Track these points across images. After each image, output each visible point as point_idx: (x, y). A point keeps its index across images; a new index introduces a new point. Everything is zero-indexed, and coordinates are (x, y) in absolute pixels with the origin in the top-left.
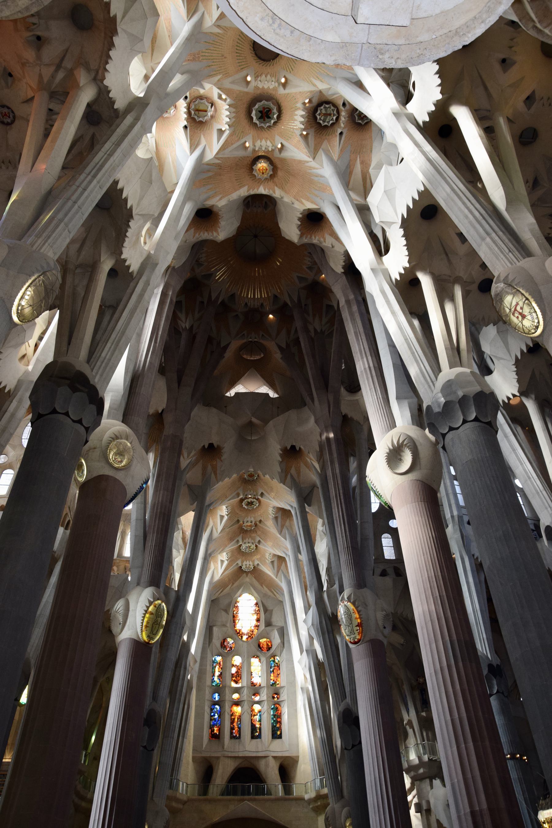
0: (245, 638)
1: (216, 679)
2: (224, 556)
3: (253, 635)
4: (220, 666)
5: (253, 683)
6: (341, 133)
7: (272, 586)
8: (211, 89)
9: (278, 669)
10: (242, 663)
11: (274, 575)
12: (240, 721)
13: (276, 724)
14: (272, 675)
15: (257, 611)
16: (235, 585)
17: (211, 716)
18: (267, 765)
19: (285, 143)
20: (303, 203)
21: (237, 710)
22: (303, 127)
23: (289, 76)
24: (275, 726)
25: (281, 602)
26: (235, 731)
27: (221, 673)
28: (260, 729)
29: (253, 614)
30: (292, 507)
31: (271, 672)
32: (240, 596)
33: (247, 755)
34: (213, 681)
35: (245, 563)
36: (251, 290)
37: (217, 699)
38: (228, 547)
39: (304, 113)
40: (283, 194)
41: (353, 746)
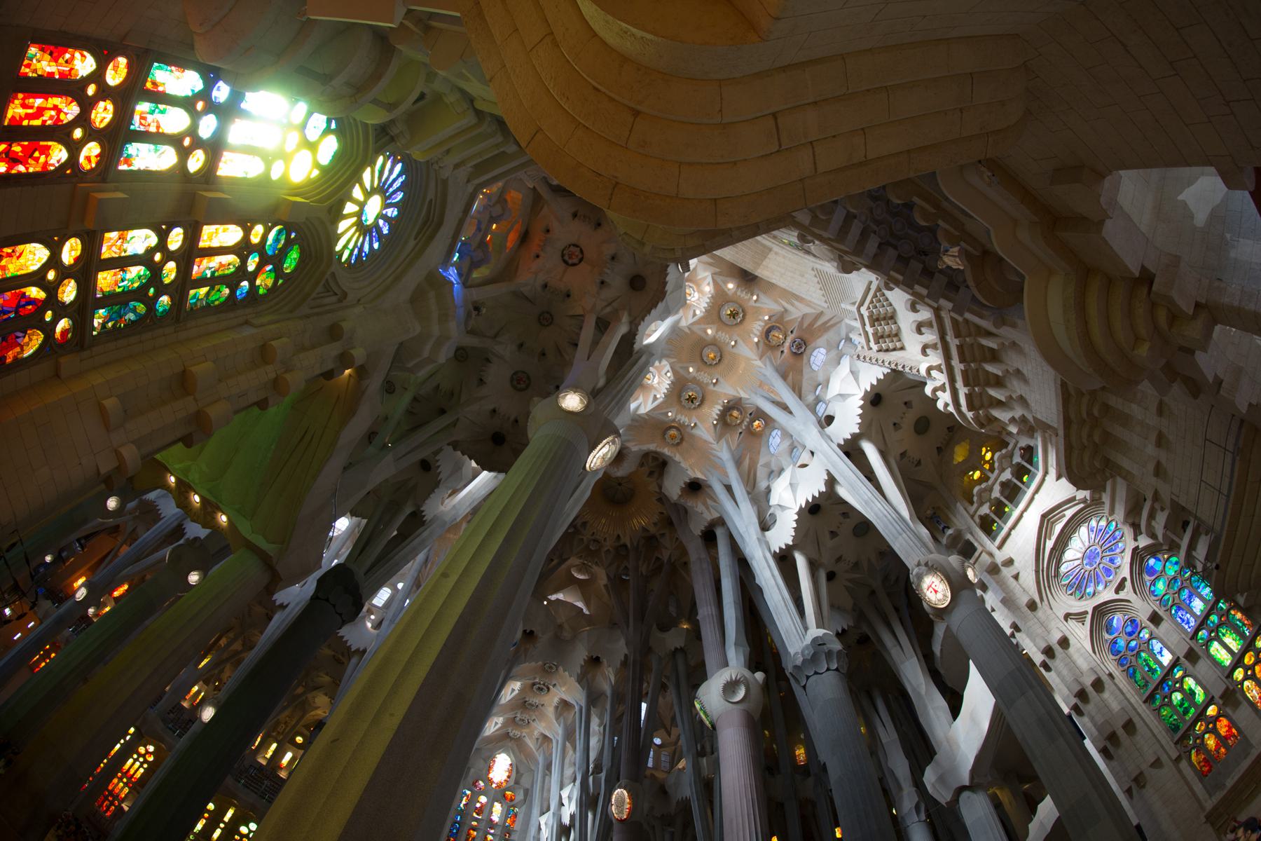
0: (494, 786)
1: (462, 805)
6: (741, 433)
7: (530, 756)
8: (665, 366)
10: (487, 803)
19: (698, 424)
20: (694, 472)
22: (717, 417)
23: (720, 379)
29: (506, 771)
30: (577, 703)
32: (499, 754)
35: (514, 731)
39: (721, 408)
40: (681, 460)
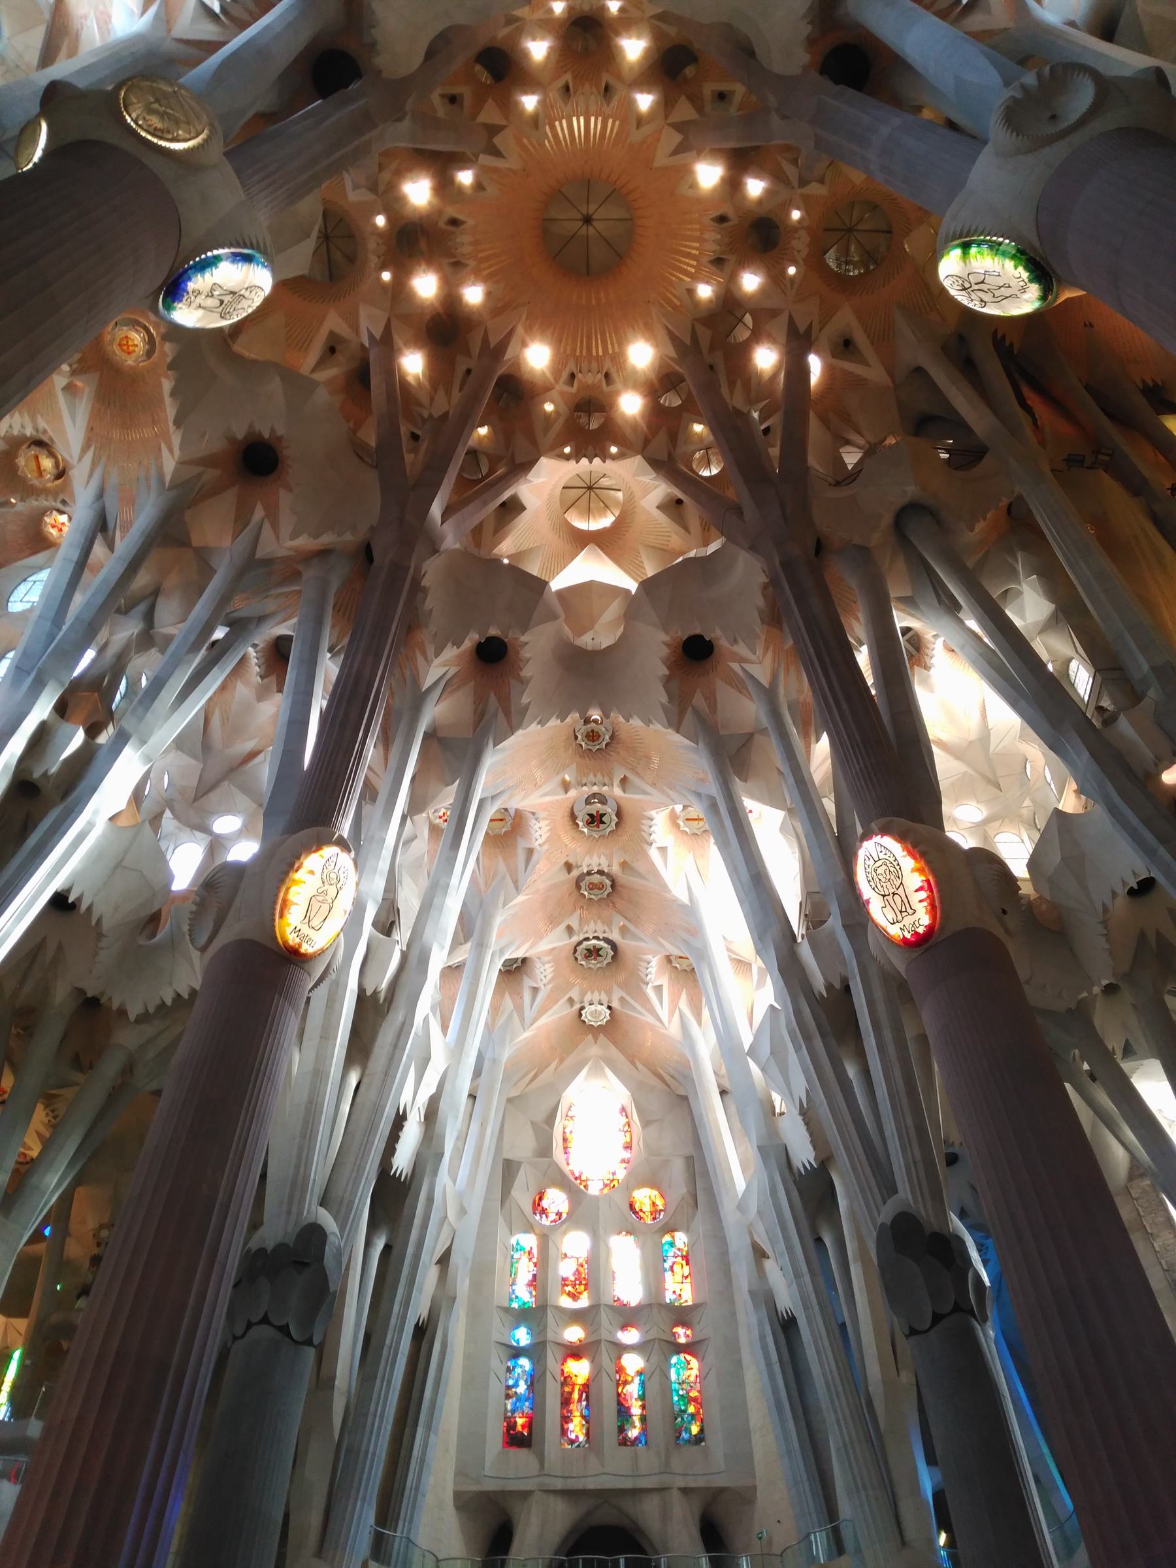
4: (530, 1259)
9: (684, 1263)
13: (686, 1405)
16: (567, 1062)
17: (508, 1388)
18: (665, 1517)
21: (580, 1370)
24: (684, 1411)
27: (534, 1276)
33: (608, 1486)
36: (582, 342)
41: (937, 1318)
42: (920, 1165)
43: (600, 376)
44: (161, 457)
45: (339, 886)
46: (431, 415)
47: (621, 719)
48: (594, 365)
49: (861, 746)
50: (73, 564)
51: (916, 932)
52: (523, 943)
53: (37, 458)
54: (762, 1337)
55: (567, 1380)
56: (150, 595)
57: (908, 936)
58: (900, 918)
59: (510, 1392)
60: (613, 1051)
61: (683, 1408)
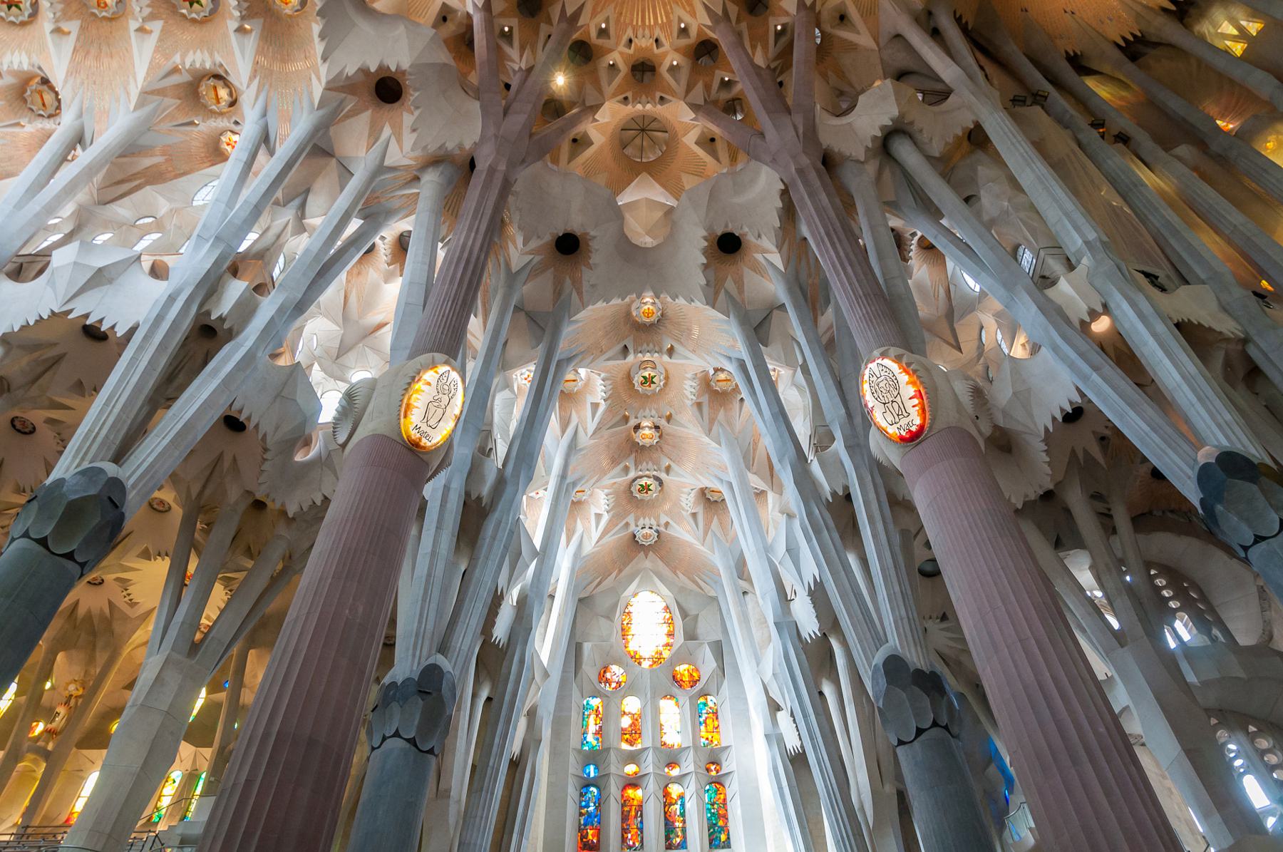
0: (646, 664)
2: (600, 502)
3: (662, 660)
4: (597, 716)
5: (665, 744)
9: (715, 718)
10: (644, 708)
11: (698, 539)
12: (641, 816)
14: (703, 728)
15: (668, 619)
16: (623, 574)
24: (715, 825)
25: (715, 599)
26: (632, 836)
27: (600, 727)
28: (684, 830)
31: (700, 723)
32: (635, 595)
34: (584, 741)
36: (638, 15)
37: (592, 775)
38: (608, 476)
41: (920, 732)
42: (906, 621)
43: (652, 41)
44: (311, 84)
45: (450, 395)
46: (520, 68)
47: (669, 299)
48: (647, 32)
49: (863, 298)
50: (243, 164)
51: (910, 431)
52: (591, 478)
53: (215, 88)
54: (775, 769)
55: (625, 802)
56: (304, 192)
57: (904, 434)
58: (897, 420)
59: (583, 811)
60: (661, 566)
61: (714, 822)
